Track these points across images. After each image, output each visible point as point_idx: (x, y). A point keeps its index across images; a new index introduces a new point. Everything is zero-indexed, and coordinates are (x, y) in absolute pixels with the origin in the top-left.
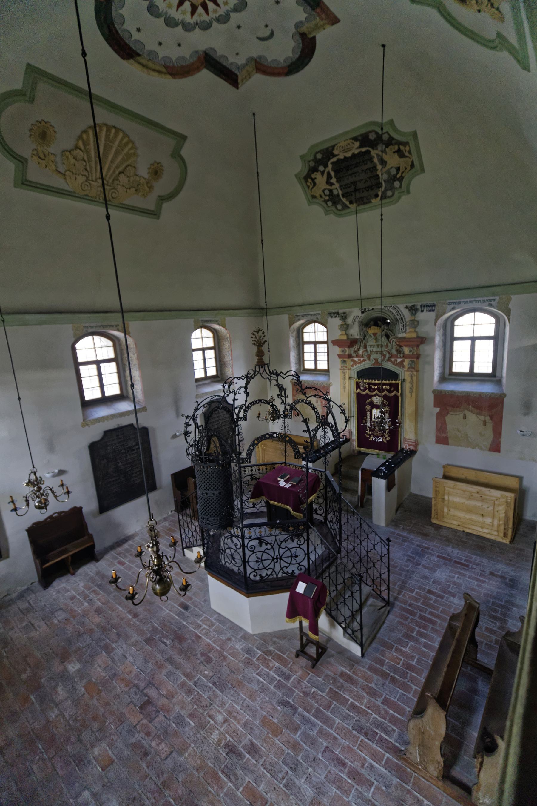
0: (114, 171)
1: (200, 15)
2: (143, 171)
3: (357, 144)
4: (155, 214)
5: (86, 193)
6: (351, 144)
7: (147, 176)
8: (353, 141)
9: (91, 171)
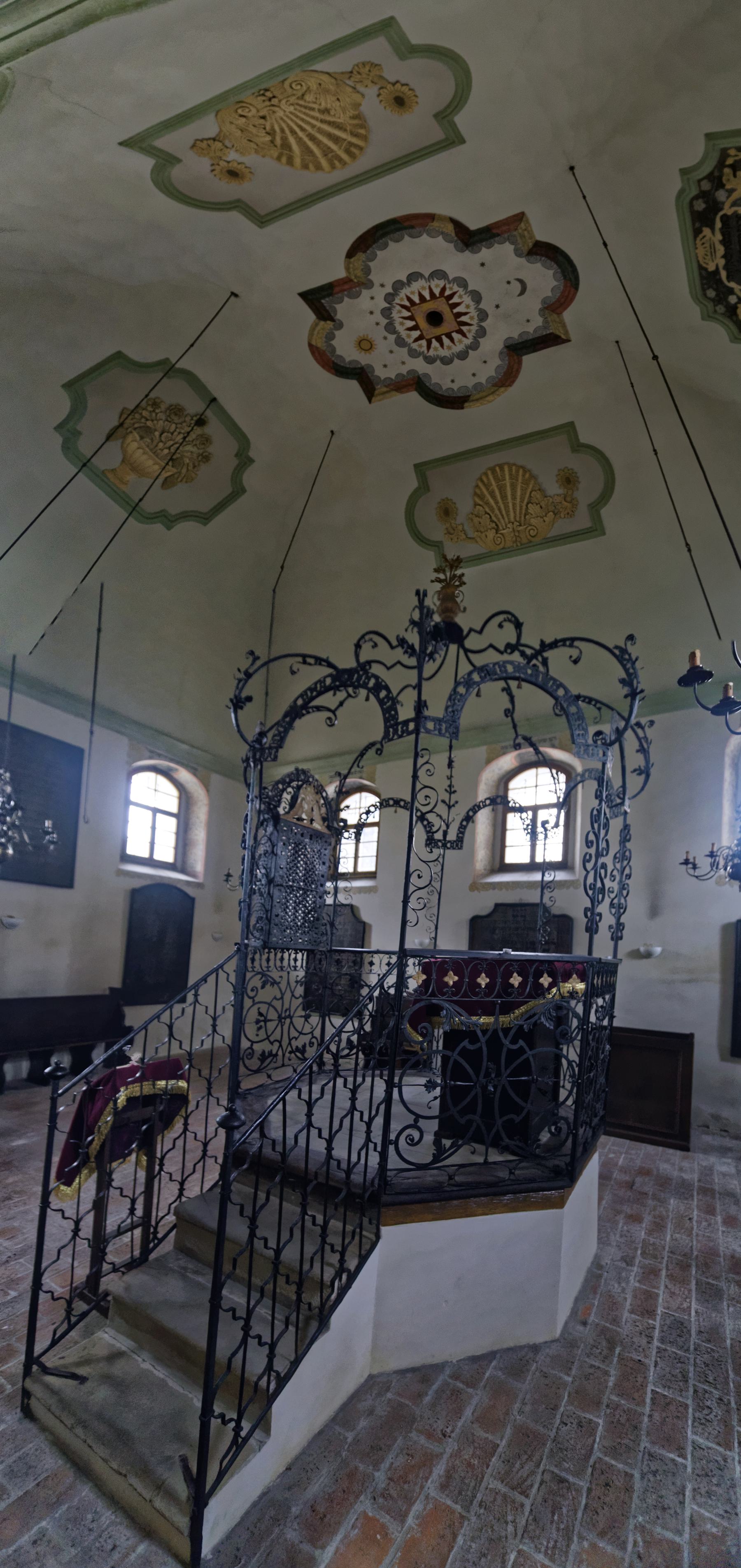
0: (521, 507)
1: (469, 331)
2: (554, 489)
3: (707, 231)
4: (596, 529)
5: (502, 546)
6: (703, 241)
7: (561, 491)
8: (701, 236)
9: (499, 520)
